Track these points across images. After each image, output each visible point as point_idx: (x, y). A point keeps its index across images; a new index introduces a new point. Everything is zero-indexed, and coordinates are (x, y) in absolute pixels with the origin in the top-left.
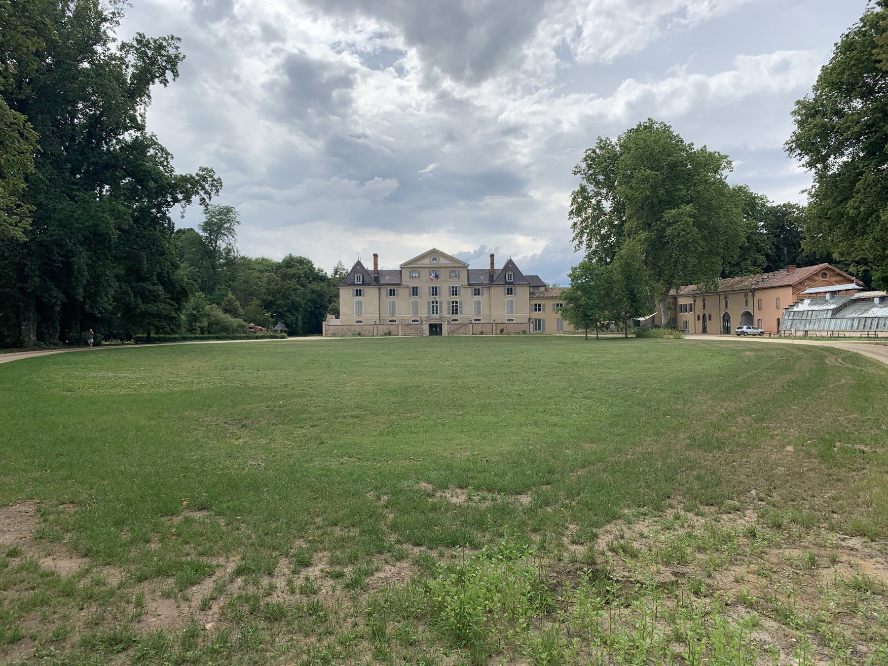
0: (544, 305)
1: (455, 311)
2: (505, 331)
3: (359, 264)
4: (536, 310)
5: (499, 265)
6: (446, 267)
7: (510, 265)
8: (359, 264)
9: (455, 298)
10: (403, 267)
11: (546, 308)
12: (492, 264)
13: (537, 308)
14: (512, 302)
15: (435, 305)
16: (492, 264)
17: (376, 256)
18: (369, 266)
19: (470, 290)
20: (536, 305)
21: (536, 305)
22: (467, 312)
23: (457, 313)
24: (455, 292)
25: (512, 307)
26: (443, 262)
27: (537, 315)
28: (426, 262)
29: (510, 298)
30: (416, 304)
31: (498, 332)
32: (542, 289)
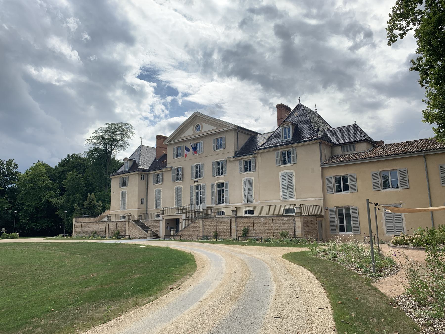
0: (353, 178)
1: (221, 200)
2: (251, 233)
4: (338, 189)
9: (221, 179)
11: (359, 183)
13: (343, 185)
14: (290, 176)
15: (199, 191)
19: (237, 163)
20: (338, 179)
21: (338, 179)
22: (236, 199)
23: (223, 202)
24: (220, 170)
25: (290, 186)
29: (286, 169)
30: (178, 190)
31: (240, 234)
32: (362, 148)
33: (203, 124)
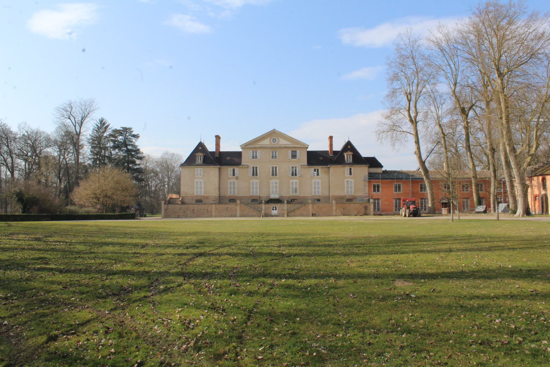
3: (201, 145)
5: (338, 147)
6: (286, 148)
7: (349, 147)
8: (201, 145)
10: (245, 146)
12: (331, 145)
16: (331, 145)
17: (218, 138)
18: (211, 147)
26: (283, 142)
27: (376, 194)
28: (266, 142)
33: (280, 139)
